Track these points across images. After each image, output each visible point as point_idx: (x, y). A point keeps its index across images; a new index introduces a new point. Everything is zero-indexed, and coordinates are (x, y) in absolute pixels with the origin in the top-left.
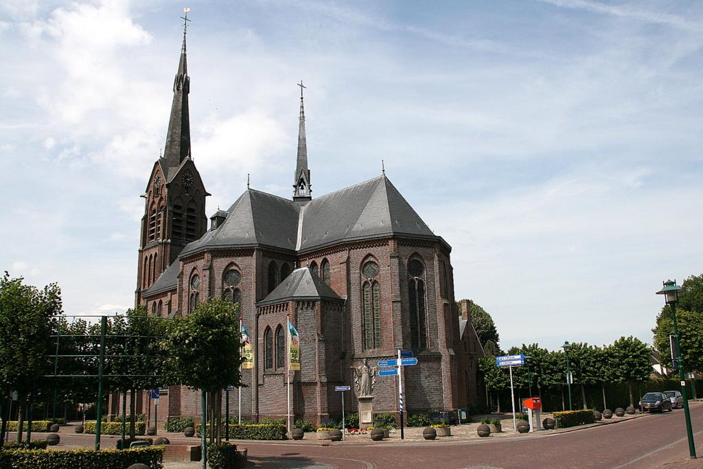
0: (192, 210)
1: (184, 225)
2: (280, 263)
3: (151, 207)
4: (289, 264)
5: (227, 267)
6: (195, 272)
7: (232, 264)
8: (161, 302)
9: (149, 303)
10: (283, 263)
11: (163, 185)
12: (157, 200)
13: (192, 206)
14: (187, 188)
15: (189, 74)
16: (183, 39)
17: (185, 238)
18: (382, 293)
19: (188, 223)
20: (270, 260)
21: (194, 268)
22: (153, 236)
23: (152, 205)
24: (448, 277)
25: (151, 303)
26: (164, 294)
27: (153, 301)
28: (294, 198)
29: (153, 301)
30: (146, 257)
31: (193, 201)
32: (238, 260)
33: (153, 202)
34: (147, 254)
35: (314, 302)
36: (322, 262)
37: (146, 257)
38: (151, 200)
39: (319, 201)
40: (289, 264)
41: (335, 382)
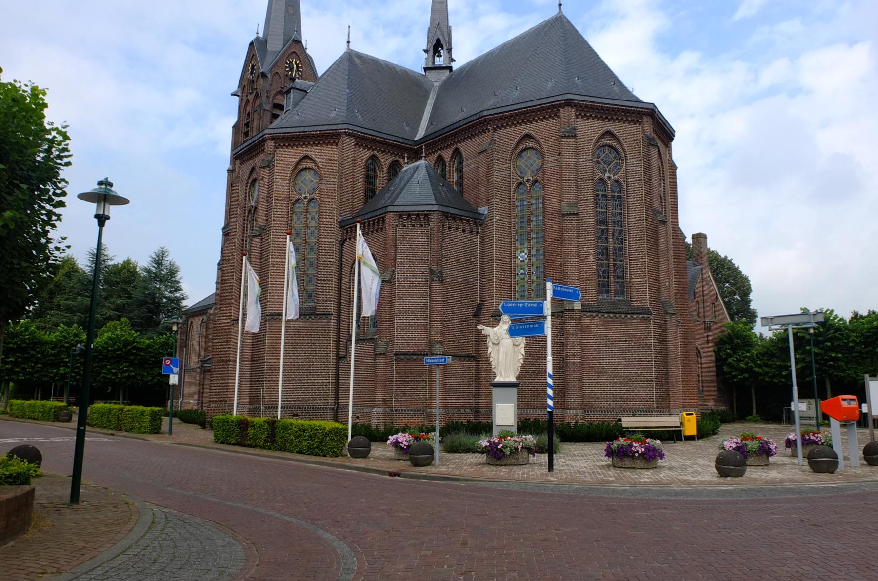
2: (386, 160)
3: (245, 108)
4: (400, 160)
5: (298, 163)
6: (254, 176)
7: (306, 157)
10: (391, 159)
11: (259, 74)
12: (251, 97)
18: (548, 201)
20: (369, 154)
21: (253, 169)
24: (668, 181)
28: (426, 69)
32: (315, 152)
33: (248, 100)
35: (427, 215)
36: (453, 154)
38: (245, 100)
39: (462, 70)
40: (400, 160)
41: (461, 356)
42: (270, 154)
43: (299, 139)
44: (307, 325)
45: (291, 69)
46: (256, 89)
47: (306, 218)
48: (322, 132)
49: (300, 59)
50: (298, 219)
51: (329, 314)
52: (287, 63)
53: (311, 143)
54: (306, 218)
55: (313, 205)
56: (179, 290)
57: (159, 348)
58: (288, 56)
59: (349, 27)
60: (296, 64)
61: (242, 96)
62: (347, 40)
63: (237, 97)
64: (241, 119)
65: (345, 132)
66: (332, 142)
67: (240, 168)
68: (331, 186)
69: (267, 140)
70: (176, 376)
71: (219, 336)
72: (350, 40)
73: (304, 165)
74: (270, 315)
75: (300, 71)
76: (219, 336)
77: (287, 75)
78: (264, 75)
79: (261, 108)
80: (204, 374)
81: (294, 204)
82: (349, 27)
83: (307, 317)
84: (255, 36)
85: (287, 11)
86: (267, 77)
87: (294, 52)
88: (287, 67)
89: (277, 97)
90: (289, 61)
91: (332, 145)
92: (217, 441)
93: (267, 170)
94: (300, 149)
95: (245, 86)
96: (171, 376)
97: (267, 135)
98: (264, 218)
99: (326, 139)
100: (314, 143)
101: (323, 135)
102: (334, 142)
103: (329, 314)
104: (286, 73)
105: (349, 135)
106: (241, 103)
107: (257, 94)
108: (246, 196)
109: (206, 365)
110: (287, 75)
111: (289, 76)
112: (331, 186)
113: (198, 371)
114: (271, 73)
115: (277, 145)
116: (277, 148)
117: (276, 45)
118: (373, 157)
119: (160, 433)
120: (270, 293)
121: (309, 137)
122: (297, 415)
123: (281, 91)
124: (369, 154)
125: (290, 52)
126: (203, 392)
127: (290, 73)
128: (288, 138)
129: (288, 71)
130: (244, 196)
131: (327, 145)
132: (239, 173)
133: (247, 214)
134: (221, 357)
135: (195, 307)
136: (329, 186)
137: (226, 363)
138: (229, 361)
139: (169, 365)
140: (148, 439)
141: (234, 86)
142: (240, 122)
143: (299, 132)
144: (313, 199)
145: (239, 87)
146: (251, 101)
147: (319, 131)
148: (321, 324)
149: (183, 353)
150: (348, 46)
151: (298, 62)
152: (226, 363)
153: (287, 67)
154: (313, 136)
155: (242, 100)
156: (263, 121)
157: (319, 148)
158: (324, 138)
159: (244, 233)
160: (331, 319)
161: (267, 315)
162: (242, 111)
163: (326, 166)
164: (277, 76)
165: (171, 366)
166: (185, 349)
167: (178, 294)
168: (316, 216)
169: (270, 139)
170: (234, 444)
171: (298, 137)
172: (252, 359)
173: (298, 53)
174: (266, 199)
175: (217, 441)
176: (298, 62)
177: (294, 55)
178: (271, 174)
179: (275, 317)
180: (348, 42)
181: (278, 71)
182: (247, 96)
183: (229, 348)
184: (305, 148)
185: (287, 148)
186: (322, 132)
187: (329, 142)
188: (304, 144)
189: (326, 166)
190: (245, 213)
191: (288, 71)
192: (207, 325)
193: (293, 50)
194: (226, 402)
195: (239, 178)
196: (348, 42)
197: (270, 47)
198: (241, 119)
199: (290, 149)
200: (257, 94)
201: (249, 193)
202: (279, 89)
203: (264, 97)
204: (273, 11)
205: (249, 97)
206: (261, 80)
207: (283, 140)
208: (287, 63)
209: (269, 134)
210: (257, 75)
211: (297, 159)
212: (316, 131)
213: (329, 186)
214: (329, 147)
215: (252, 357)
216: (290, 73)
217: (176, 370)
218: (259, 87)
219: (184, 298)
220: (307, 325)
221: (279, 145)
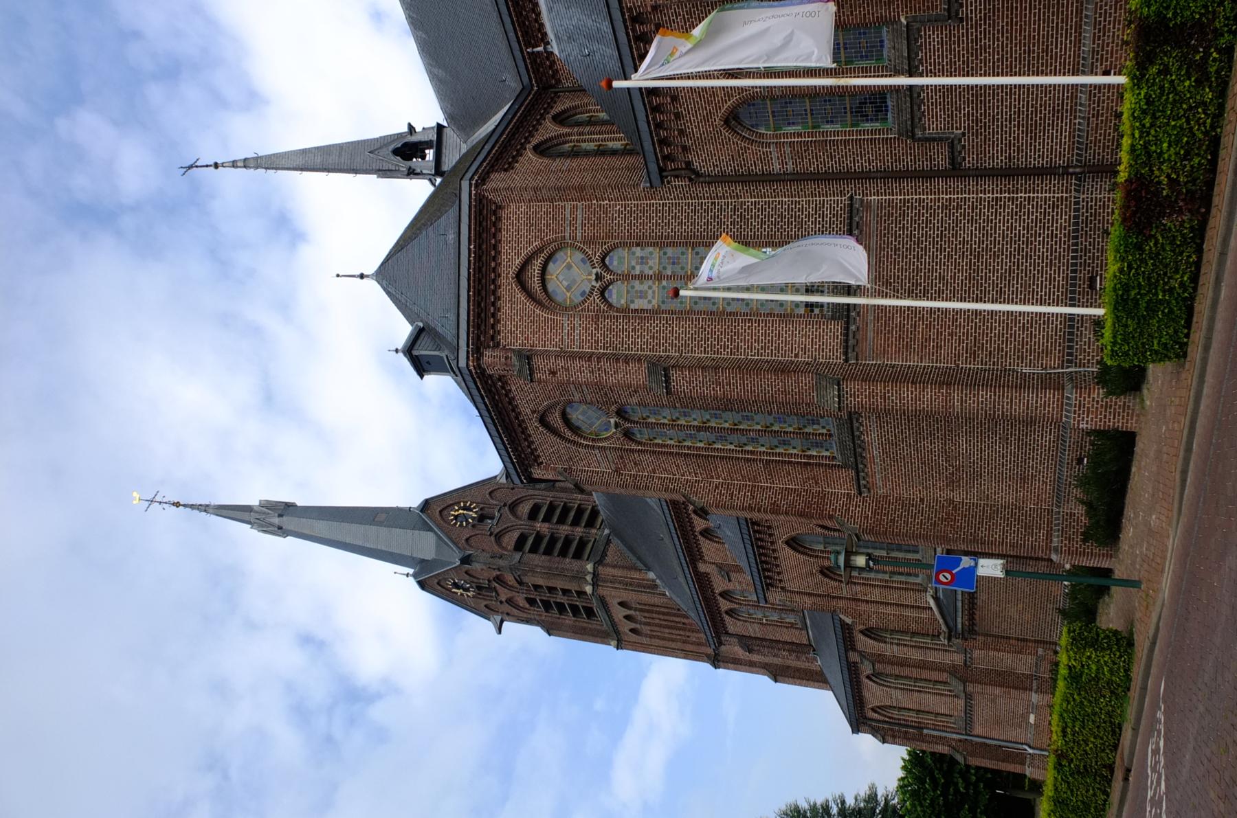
0: (533, 515)
1: (565, 530)
8: (725, 595)
9: (730, 631)
12: (504, 594)
13: (525, 509)
14: (482, 518)
15: (254, 501)
16: (188, 510)
17: (594, 531)
19: (562, 521)
22: (570, 605)
25: (732, 625)
26: (702, 581)
27: (727, 618)
29: (727, 618)
30: (632, 630)
31: (513, 507)
33: (509, 601)
34: (625, 627)
38: (507, 608)
42: (507, 358)
43: (483, 293)
45: (466, 518)
46: (489, 581)
47: (642, 277)
48: (473, 238)
50: (642, 295)
51: (851, 205)
52: (455, 524)
53: (493, 264)
54: (642, 277)
55: (615, 263)
56: (827, 806)
57: (921, 805)
58: (445, 522)
59: (338, 276)
60: (458, 510)
61: (502, 613)
62: (359, 279)
63: (505, 624)
64: (537, 618)
65: (477, 186)
66: (493, 218)
68: (580, 217)
69: (479, 365)
70: (982, 562)
71: (893, 521)
72: (359, 273)
73: (535, 284)
74: (846, 353)
75: (470, 505)
76: (893, 521)
77: (473, 526)
78: (466, 560)
79: (518, 569)
80: (975, 633)
82: (338, 276)
84: (411, 579)
85: (380, 524)
86: (470, 555)
87: (441, 512)
88: (461, 525)
89: (504, 545)
90: (452, 520)
91: (499, 219)
92: (1177, 351)
93: (538, 362)
94: (502, 292)
95: (486, 606)
96: (981, 572)
97: (471, 364)
98: (633, 366)
99: (487, 230)
100: (494, 259)
101: (479, 235)
102: (495, 213)
103: (851, 205)
104: (470, 526)
105: (483, 180)
106: (513, 616)
107: (498, 579)
108: (599, 448)
109: (960, 626)
110: (473, 526)
112: (580, 217)
113: (970, 688)
114: (465, 549)
115: (491, 344)
116: (498, 344)
117: (426, 544)
118: (536, 149)
119: (1131, 633)
120: (796, 356)
122: (1092, 281)
123: (496, 536)
124: (529, 154)
125: (439, 518)
126: (1018, 639)
127: (470, 520)
128: (479, 315)
129: (468, 523)
130: (597, 452)
131: (500, 230)
132: (555, 469)
133: (634, 446)
134: (941, 519)
135: (844, 703)
136: (579, 222)
137: (955, 509)
140: (1152, 632)
142: (543, 621)
143: (469, 291)
145: (488, 619)
146: (510, 594)
147: (470, 244)
148: (874, 225)
149: (933, 736)
150: (368, 276)
151: (457, 508)
152: (955, 509)
153: (461, 525)
154: (479, 258)
155: (508, 614)
156: (536, 566)
157: (504, 248)
159: (671, 453)
160: (862, 201)
161: (846, 360)
162: (525, 615)
163: (540, 230)
164: (472, 541)
166: (925, 731)
167: (835, 810)
168: (638, 251)
169: (478, 359)
170: (1200, 251)
171: (478, 293)
172: (948, 384)
173: (443, 506)
175: (1177, 351)
176: (457, 508)
177: (445, 513)
178: (546, 354)
179: (851, 342)
180: (362, 276)
181: (465, 538)
182: (501, 602)
184: (502, 281)
185: (499, 321)
186: (473, 238)
187: (494, 224)
189: (540, 230)
190: (632, 451)
191: (468, 523)
192: (879, 662)
193: (438, 513)
194: (1050, 512)
195: (565, 470)
196: (362, 276)
197: (430, 555)
198: (537, 618)
199: (502, 315)
200: (498, 579)
201: (593, 440)
202: (493, 538)
203: (501, 563)
204: (379, 548)
205: (504, 600)
206: (476, 567)
207: (483, 328)
208: (455, 524)
209: (468, 358)
210: (467, 577)
211: (521, 297)
212: (469, 250)
213: (579, 222)
215: (941, 384)
216: (470, 520)
217: (966, 562)
218: (486, 575)
219: (843, 802)
221: (493, 338)
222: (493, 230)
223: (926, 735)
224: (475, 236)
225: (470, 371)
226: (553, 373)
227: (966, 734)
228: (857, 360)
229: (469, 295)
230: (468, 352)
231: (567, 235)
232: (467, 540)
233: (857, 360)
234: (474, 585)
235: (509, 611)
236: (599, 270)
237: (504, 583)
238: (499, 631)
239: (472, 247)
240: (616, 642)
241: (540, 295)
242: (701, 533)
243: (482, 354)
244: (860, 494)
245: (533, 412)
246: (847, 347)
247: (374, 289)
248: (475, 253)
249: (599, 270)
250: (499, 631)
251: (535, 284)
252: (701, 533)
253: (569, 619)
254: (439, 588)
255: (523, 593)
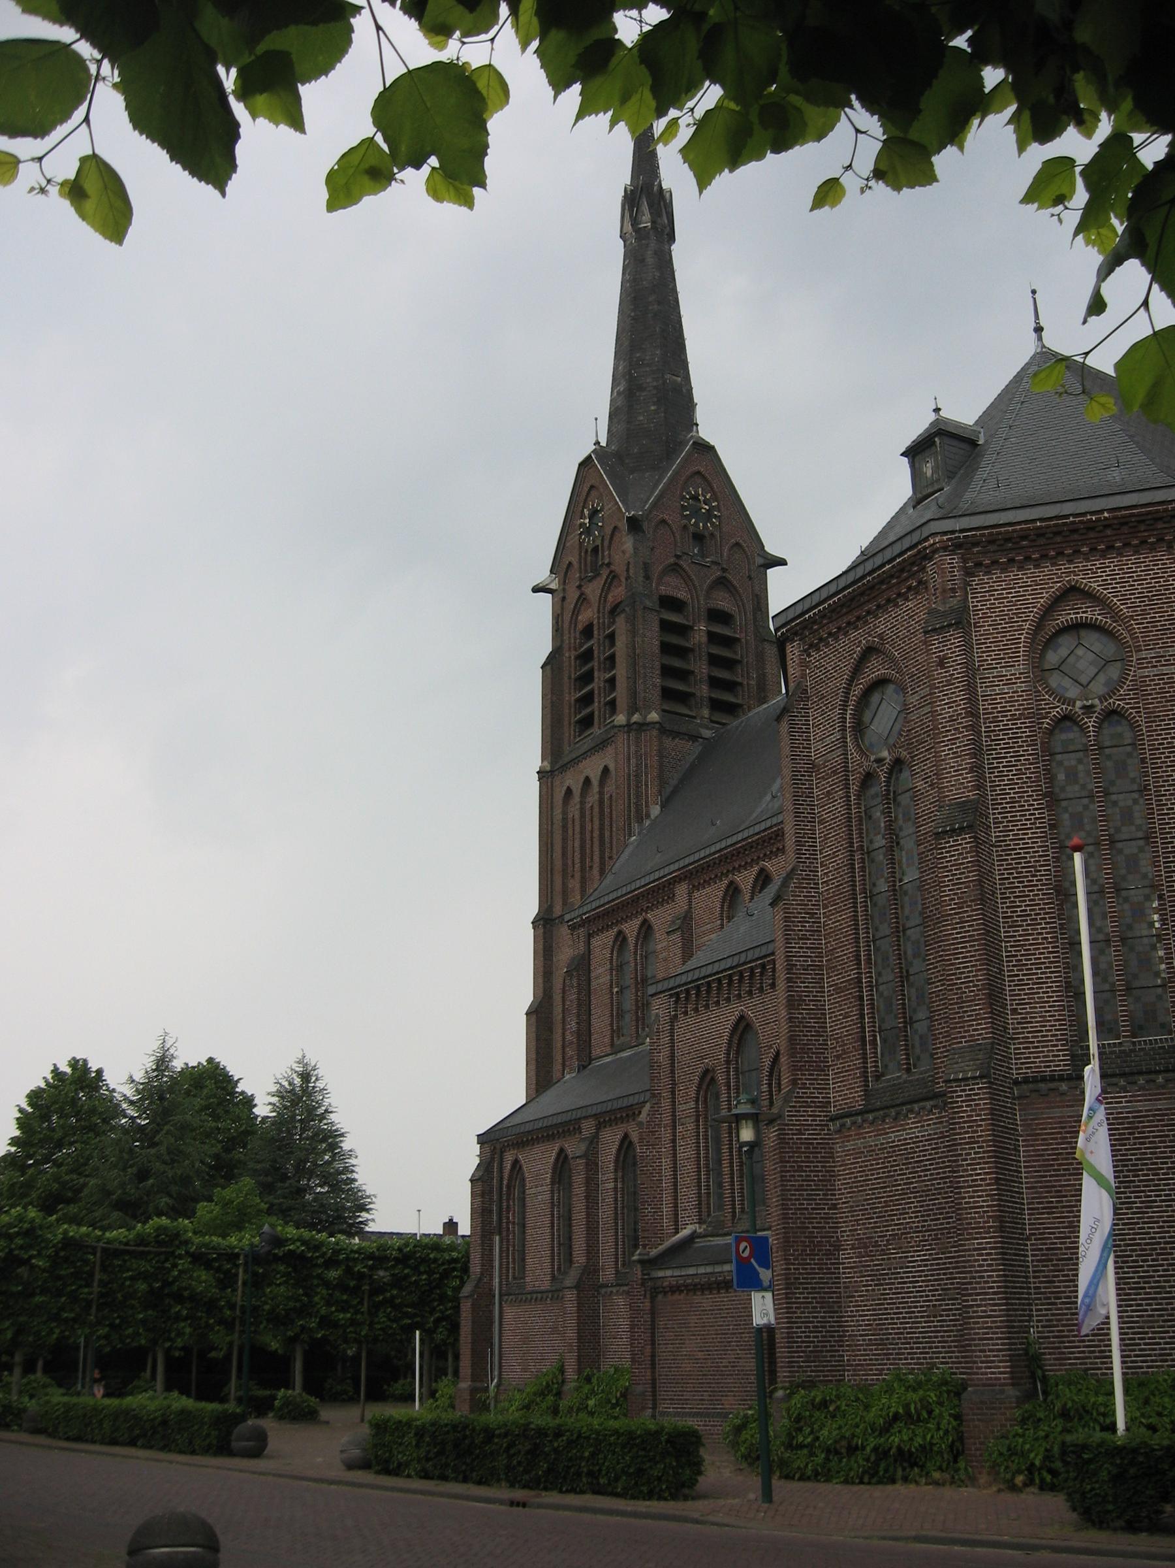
0: (718, 616)
1: (701, 668)
8: (646, 929)
9: (596, 942)
12: (593, 590)
13: (723, 602)
14: (698, 538)
17: (706, 712)
19: (714, 660)
22: (591, 693)
23: (576, 612)
25: (602, 943)
26: (660, 893)
27: (613, 932)
29: (613, 932)
30: (569, 791)
31: (722, 583)
33: (582, 599)
34: (573, 780)
37: (569, 791)
38: (573, 595)
42: (953, 590)
43: (1042, 541)
44: (1161, 1105)
46: (609, 565)
49: (712, 488)
59: (1034, 292)
61: (564, 590)
62: (1033, 325)
67: (804, 664)
69: (934, 552)
73: (1067, 616)
74: (1026, 1081)
81: (1050, 732)
82: (1034, 292)
83: (1160, 1080)
87: (699, 473)
88: (684, 508)
89: (666, 579)
91: (1153, 548)
93: (955, 638)
94: (1047, 569)
95: (570, 564)
101: (1124, 522)
104: (685, 521)
107: (613, 577)
109: (661, 1274)
110: (685, 527)
111: (691, 529)
120: (1014, 1011)
121: (1074, 531)
123: (676, 564)
126: (653, 1356)
129: (689, 518)
131: (1136, 552)
132: (804, 676)
133: (854, 788)
136: (1165, 670)
137: (829, 1254)
138: (838, 1247)
139: (748, 1258)
141: (542, 571)
143: (1041, 520)
144: (1114, 712)
147: (1109, 511)
149: (491, 1250)
150: (1040, 339)
152: (829, 1254)
153: (684, 508)
154: (1090, 527)
155: (564, 599)
157: (1112, 563)
158: (1125, 529)
161: (1016, 1082)
162: (566, 625)
163: (1144, 613)
165: (752, 1260)
169: (945, 549)
172: (1001, 1229)
174: (967, 721)
177: (699, 480)
178: (968, 648)
179: (1042, 1086)
180: (1039, 330)
183: (834, 1207)
185: (1003, 570)
187: (1144, 542)
188: (1060, 554)
189: (1144, 613)
191: (689, 518)
192: (587, 1164)
196: (1039, 330)
202: (672, 560)
207: (992, 548)
209: (945, 533)
210: (608, 531)
211: (1044, 598)
212: (1102, 511)
213: (1165, 670)
214: (1146, 558)
215: (1000, 1219)
220: (1161, 1105)
221: (978, 564)
222: (1136, 542)
223: (491, 1240)
224: (1124, 517)
225: (926, 539)
226: (941, 663)
227: (501, 1295)
228: (1019, 1098)
229: (1034, 521)
230: (953, 532)
231: (1143, 654)
232: (664, 521)
233: (1019, 1098)
234: (598, 542)
235: (568, 601)
236: (1098, 709)
237: (609, 588)
238: (536, 590)
239: (1106, 515)
240: (548, 768)
241: (1052, 626)
242: (731, 883)
243: (953, 552)
244: (832, 1119)
245: (881, 636)
246: (1035, 1080)
247: (1024, 351)
248: (1098, 520)
249: (1098, 709)
250: (536, 590)
251: (1067, 616)
252: (731, 883)
253: (571, 696)
254: (586, 489)
255: (599, 618)
